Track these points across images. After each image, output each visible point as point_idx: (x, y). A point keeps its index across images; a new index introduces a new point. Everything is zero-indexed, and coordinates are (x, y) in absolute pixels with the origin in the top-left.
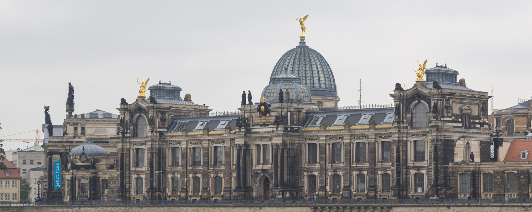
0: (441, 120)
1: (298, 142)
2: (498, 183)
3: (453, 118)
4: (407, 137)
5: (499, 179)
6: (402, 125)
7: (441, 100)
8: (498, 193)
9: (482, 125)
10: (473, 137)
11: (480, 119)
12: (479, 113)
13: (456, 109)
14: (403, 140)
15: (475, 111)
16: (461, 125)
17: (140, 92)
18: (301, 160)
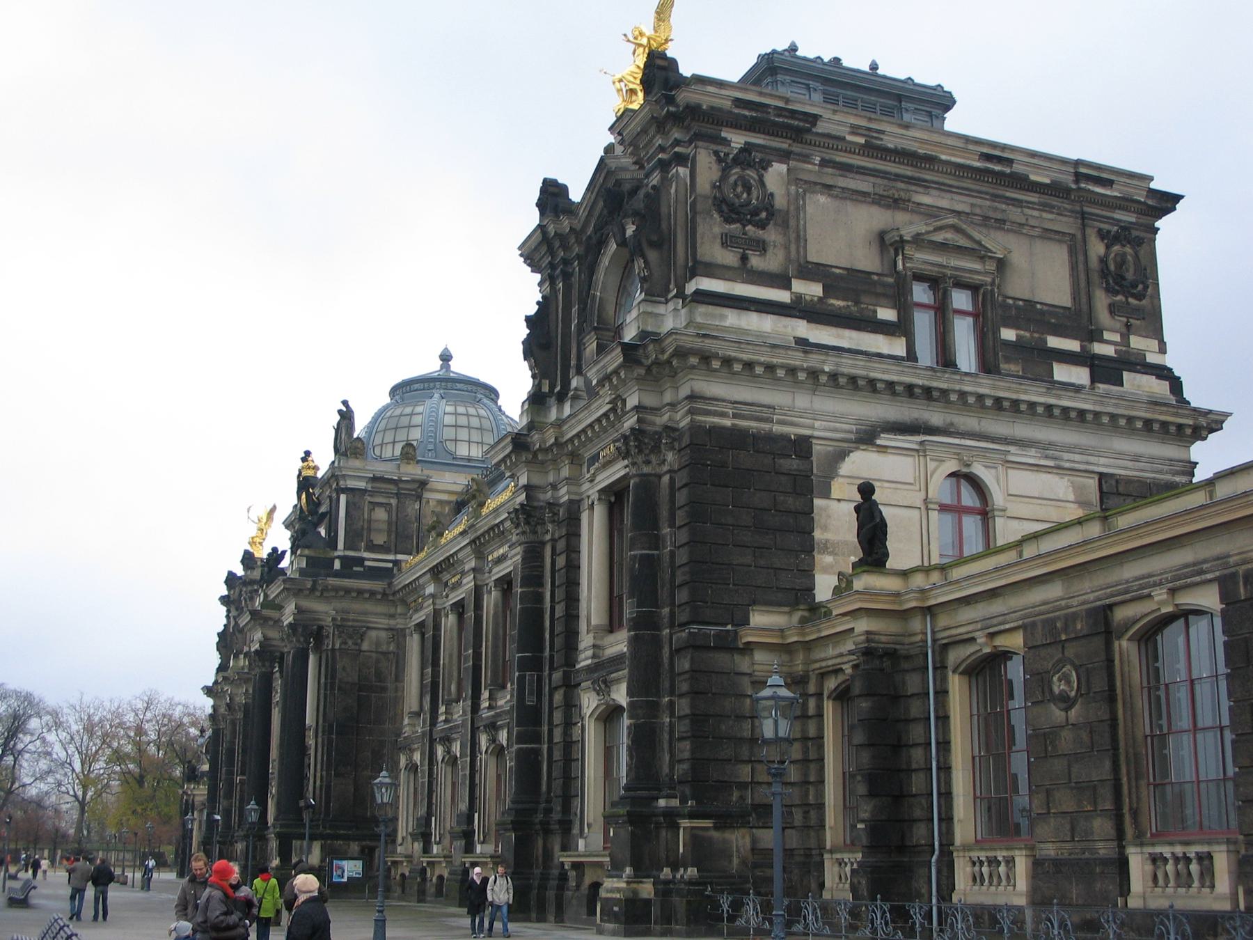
0: (681, 294)
1: (384, 622)
2: (1066, 741)
3: (813, 290)
4: (573, 481)
5: (1066, 702)
6: (553, 415)
7: (681, 159)
8: (958, 840)
9: (1107, 371)
10: (1022, 443)
11: (1094, 335)
12: (1081, 290)
13: (842, 233)
14: (552, 505)
15: (1044, 275)
16: (897, 347)
17: (252, 543)
18: (398, 700)
